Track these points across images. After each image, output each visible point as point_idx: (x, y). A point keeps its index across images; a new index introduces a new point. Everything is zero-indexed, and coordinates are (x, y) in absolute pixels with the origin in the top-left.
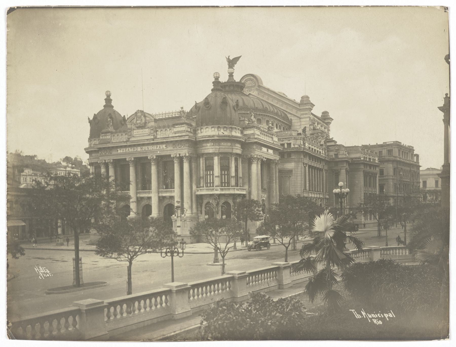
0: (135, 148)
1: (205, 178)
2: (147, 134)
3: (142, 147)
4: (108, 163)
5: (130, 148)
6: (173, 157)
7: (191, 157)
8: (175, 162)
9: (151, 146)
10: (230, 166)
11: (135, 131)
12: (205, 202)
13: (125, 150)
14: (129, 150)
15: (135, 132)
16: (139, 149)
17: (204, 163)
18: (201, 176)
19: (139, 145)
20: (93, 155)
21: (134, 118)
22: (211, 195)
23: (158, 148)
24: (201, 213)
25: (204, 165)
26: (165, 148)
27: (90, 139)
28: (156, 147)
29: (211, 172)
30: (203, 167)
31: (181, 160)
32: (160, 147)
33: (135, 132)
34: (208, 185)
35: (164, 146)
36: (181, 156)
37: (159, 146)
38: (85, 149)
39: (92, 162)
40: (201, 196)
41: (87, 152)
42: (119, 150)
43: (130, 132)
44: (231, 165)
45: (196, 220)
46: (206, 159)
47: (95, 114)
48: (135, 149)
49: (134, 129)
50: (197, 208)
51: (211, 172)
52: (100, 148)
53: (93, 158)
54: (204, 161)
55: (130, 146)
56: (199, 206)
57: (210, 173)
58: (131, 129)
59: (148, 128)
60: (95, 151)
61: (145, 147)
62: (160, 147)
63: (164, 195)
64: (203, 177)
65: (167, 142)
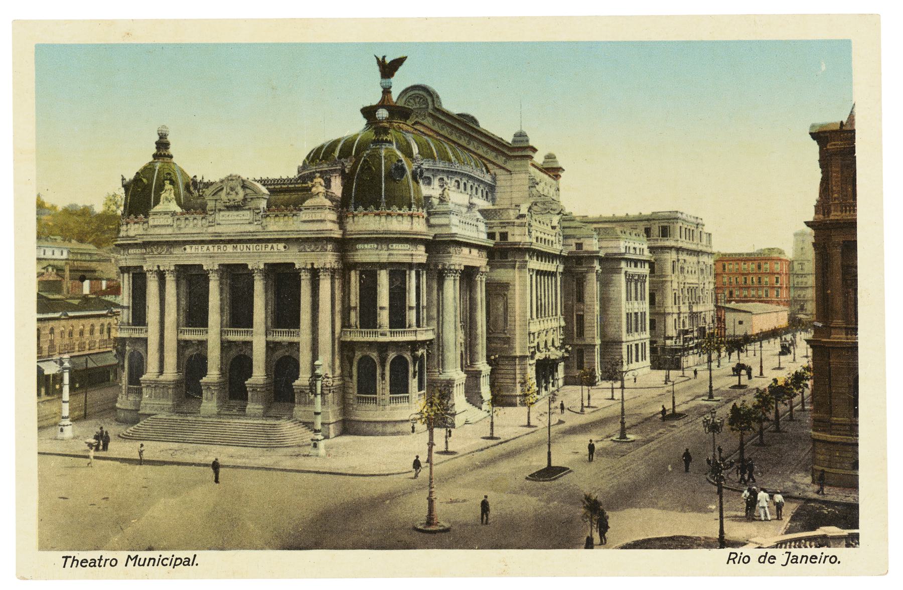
1: (358, 308)
3: (235, 245)
7: (333, 269)
9: (255, 245)
12: (358, 355)
14: (208, 249)
16: (230, 248)
18: (353, 304)
19: (230, 242)
21: (223, 189)
22: (371, 344)
23: (268, 249)
28: (263, 248)
31: (315, 274)
32: (272, 247)
35: (281, 246)
37: (270, 245)
42: (187, 247)
48: (222, 248)
49: (220, 210)
56: (347, 362)
59: (250, 209)
61: (242, 245)
62: (272, 247)
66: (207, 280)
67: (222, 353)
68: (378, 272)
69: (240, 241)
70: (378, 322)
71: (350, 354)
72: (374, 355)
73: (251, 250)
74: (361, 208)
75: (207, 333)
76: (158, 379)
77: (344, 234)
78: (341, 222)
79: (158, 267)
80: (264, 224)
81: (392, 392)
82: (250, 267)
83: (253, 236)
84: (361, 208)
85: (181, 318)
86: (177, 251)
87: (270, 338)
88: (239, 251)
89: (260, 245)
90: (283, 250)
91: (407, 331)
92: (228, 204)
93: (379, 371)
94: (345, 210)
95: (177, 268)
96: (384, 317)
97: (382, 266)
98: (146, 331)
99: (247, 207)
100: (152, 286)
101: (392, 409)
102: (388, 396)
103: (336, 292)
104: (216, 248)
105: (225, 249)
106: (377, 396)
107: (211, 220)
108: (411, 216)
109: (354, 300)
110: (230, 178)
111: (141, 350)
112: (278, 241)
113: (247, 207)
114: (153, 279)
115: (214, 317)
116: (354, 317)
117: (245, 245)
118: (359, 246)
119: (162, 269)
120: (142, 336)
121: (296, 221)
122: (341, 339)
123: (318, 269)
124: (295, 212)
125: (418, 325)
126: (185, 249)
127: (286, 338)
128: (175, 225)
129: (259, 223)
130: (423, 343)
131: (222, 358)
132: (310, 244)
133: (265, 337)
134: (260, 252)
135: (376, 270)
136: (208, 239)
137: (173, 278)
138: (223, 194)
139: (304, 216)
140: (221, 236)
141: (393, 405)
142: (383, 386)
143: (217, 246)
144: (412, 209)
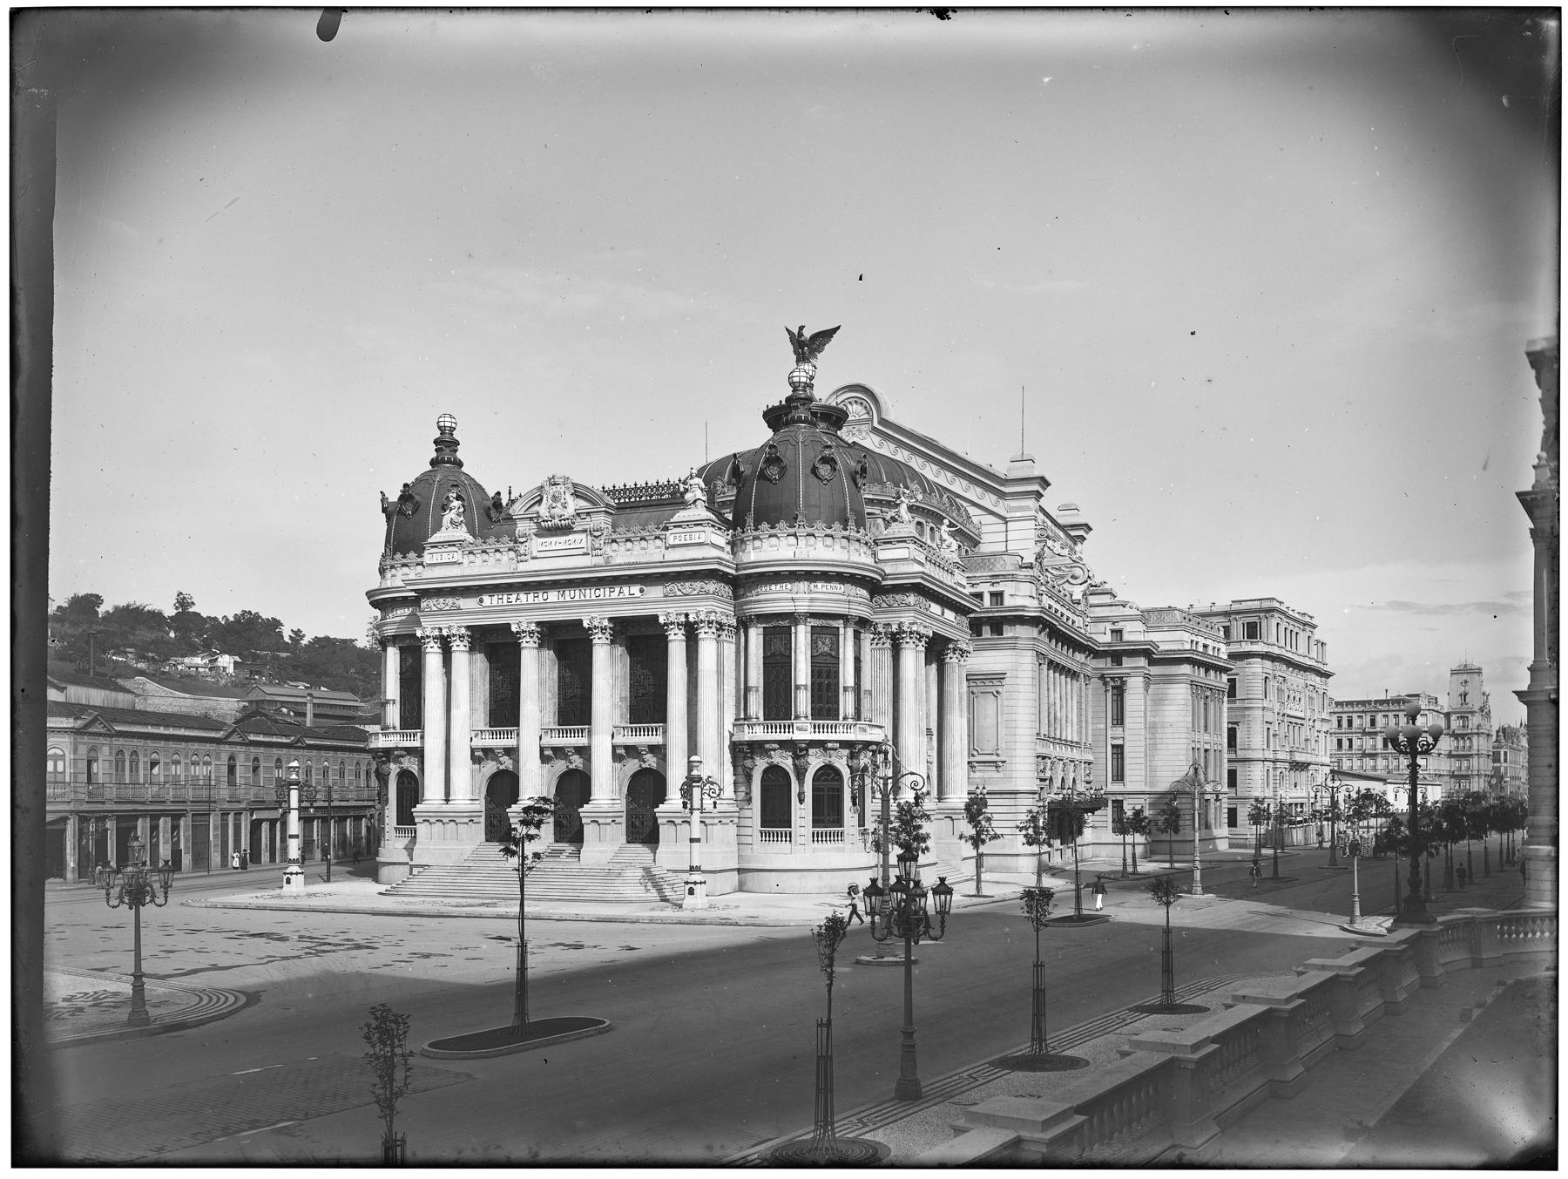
1: (761, 690)
2: (581, 551)
16: (553, 596)
23: (615, 595)
26: (638, 594)
31: (691, 632)
35: (635, 589)
36: (691, 619)
38: (369, 594)
41: (375, 604)
46: (767, 634)
47: (406, 485)
72: (787, 763)
74: (765, 526)
84: (765, 526)
96: (803, 702)
109: (756, 677)
116: (756, 706)
126: (481, 601)
139: (672, 537)
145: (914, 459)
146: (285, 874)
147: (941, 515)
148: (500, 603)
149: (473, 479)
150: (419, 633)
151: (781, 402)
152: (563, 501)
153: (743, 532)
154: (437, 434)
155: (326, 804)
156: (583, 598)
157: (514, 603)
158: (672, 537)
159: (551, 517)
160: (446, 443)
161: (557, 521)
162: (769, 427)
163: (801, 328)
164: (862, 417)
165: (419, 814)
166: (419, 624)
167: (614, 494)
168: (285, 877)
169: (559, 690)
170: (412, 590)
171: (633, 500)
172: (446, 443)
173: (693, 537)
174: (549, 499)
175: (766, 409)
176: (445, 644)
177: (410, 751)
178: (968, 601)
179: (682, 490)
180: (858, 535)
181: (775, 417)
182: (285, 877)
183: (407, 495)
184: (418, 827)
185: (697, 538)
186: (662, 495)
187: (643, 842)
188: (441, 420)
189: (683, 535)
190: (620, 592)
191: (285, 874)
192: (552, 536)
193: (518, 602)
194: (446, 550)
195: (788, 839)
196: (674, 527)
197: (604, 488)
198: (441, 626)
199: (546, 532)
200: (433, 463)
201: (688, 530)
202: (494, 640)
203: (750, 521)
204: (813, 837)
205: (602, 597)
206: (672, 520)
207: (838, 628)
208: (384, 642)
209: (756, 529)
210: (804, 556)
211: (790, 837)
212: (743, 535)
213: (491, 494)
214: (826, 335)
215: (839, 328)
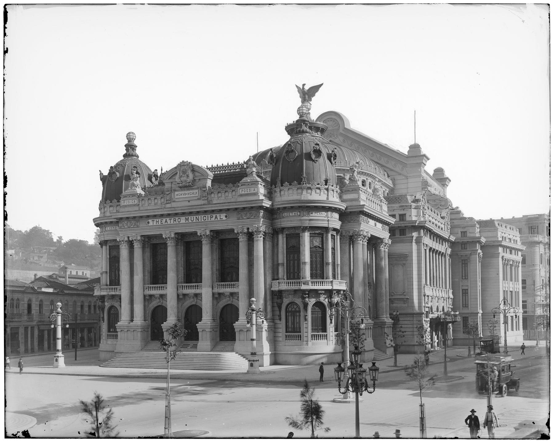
0: (177, 218)
1: (285, 265)
3: (187, 217)
4: (132, 240)
5: (168, 219)
6: (238, 233)
8: (240, 240)
9: (202, 216)
10: (325, 247)
11: (176, 193)
12: (286, 301)
13: (160, 221)
14: (166, 221)
15: (179, 195)
16: (183, 220)
17: (285, 243)
18: (280, 261)
19: (183, 214)
20: (108, 228)
22: (295, 291)
23: (213, 219)
24: (280, 319)
25: (285, 246)
27: (103, 205)
28: (209, 218)
29: (296, 256)
30: (283, 248)
31: (250, 236)
32: (216, 217)
33: (177, 195)
34: (290, 275)
35: (223, 216)
36: (250, 231)
37: (214, 216)
38: (95, 220)
39: (106, 239)
40: (280, 292)
41: (97, 225)
42: (150, 221)
43: (170, 194)
44: (326, 245)
45: (271, 330)
46: (288, 237)
47: (111, 167)
49: (175, 190)
50: (273, 311)
51: (296, 256)
52: (121, 219)
53: (108, 234)
54: (285, 239)
55: (169, 215)
56: (277, 309)
57: (294, 257)
58: (172, 190)
59: (198, 188)
60: (111, 222)
61: (192, 217)
62: (216, 217)
63: (222, 290)
64: (283, 264)
65: (228, 210)
66: (165, 245)
67: (178, 304)
68: (301, 235)
69: (191, 213)
70: (301, 274)
71: (279, 301)
72: (299, 301)
73: (200, 221)
75: (166, 288)
76: (129, 325)
77: (272, 205)
78: (270, 195)
79: (128, 237)
80: (210, 199)
81: (313, 330)
82: (199, 234)
83: (200, 208)
85: (146, 278)
86: (142, 224)
87: (216, 290)
88: (190, 221)
89: (207, 216)
90: (224, 218)
91: (324, 281)
92: (181, 185)
93: (302, 314)
94: (273, 186)
95: (143, 239)
96: (307, 271)
97: (304, 229)
98: (120, 290)
99: (196, 187)
100: (124, 252)
101: (313, 344)
102: (310, 333)
103: (267, 252)
104: (172, 221)
105: (179, 221)
106: (301, 334)
107: (168, 199)
108: (327, 189)
109: (282, 258)
110: (182, 164)
111: (116, 305)
112: (220, 211)
113: (196, 187)
114: (124, 247)
115: (171, 275)
116: (282, 271)
117: (195, 217)
118: (285, 214)
119: (130, 239)
120: (117, 293)
121: (235, 195)
122: (272, 289)
123: (252, 232)
124: (234, 188)
125: (334, 277)
126: (148, 223)
127: (228, 290)
128: (140, 204)
129: (206, 198)
130: (338, 291)
131: (178, 308)
132: (245, 212)
133: (211, 289)
134: (207, 222)
135: (299, 233)
136: (166, 213)
137: (139, 246)
138: (177, 178)
140: (176, 210)
141: (315, 341)
142: (307, 327)
143: (173, 218)
144: (328, 184)
145: (360, 148)
146: (55, 357)
147: (374, 176)
148: (157, 224)
149: (144, 164)
150: (118, 240)
151: (294, 122)
152: (187, 174)
153: (276, 187)
154: (126, 142)
155: (74, 322)
156: (197, 220)
157: (164, 224)
158: (241, 190)
159: (181, 181)
160: (130, 147)
161: (184, 184)
162: (289, 134)
163: (304, 85)
164: (334, 128)
165: (119, 327)
166: (118, 234)
167: (212, 169)
168: (55, 358)
169: (186, 266)
170: (115, 218)
171: (221, 172)
172: (130, 147)
173: (251, 190)
174: (181, 173)
175: (286, 125)
176: (131, 244)
177: (113, 297)
178: (388, 219)
179: (245, 167)
180: (333, 188)
181: (292, 129)
182: (55, 358)
183: (112, 171)
184: (119, 334)
185: (253, 190)
186: (235, 169)
187: (227, 340)
188: (128, 135)
189: (246, 189)
190: (215, 218)
191: (55, 357)
192: (182, 190)
193: (166, 223)
194: (131, 198)
195: (299, 338)
196: (242, 185)
197: (207, 166)
198: (129, 236)
199: (180, 189)
200: (125, 156)
201: (249, 186)
202: (155, 241)
203: (279, 183)
204: (312, 337)
205: (207, 220)
206: (240, 182)
207: (323, 234)
208: (103, 243)
209: (282, 186)
210: (305, 199)
211: (301, 337)
212: (276, 189)
213: (153, 171)
214: (315, 89)
215: (322, 84)
